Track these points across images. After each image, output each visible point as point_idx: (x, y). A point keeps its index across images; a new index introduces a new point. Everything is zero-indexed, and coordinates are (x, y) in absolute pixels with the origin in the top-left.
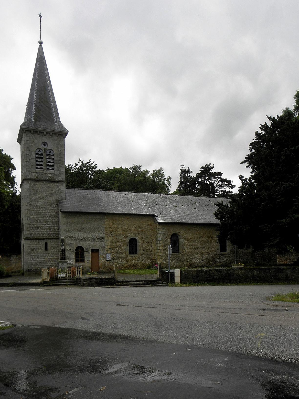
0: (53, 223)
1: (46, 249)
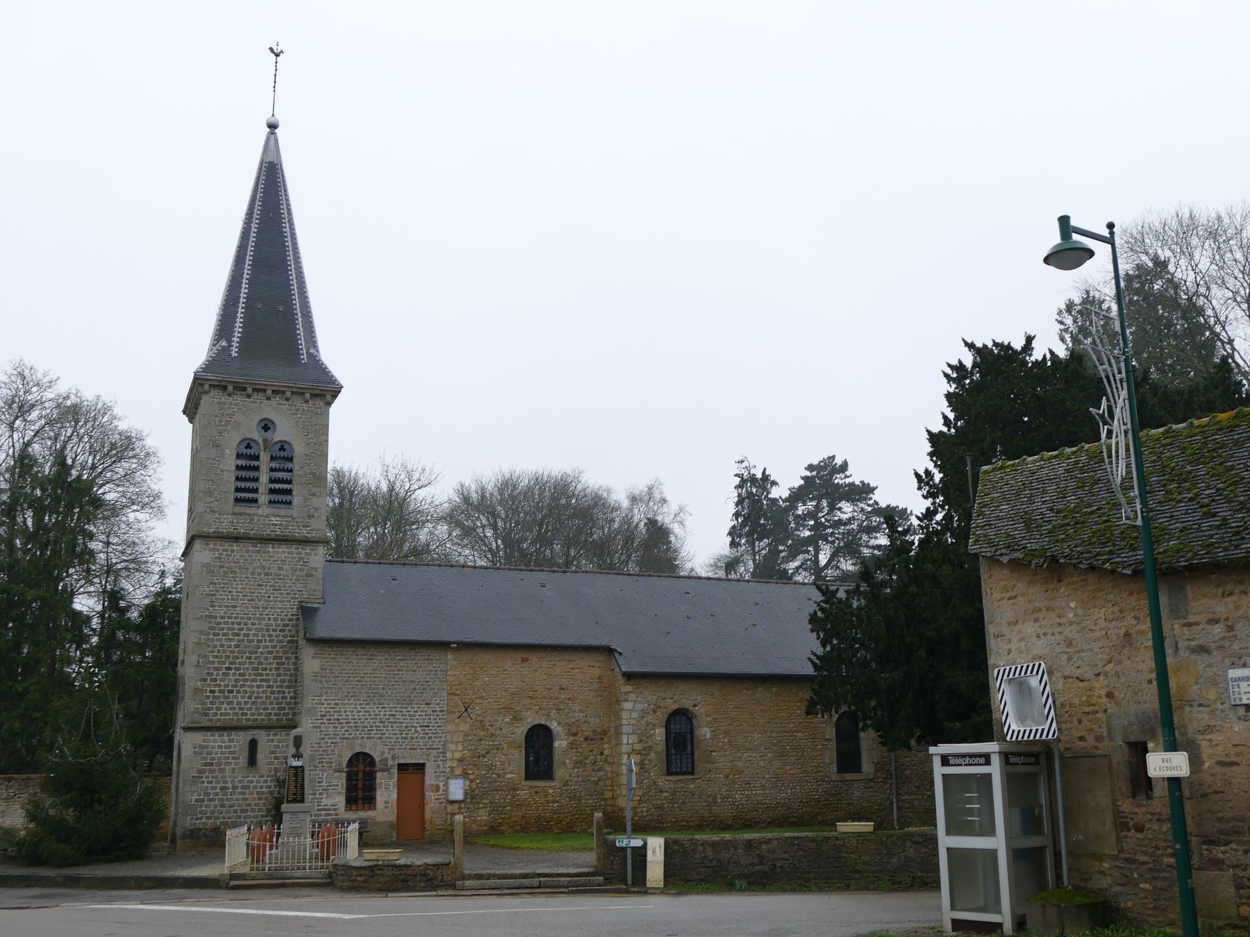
0: (279, 675)
1: (252, 761)
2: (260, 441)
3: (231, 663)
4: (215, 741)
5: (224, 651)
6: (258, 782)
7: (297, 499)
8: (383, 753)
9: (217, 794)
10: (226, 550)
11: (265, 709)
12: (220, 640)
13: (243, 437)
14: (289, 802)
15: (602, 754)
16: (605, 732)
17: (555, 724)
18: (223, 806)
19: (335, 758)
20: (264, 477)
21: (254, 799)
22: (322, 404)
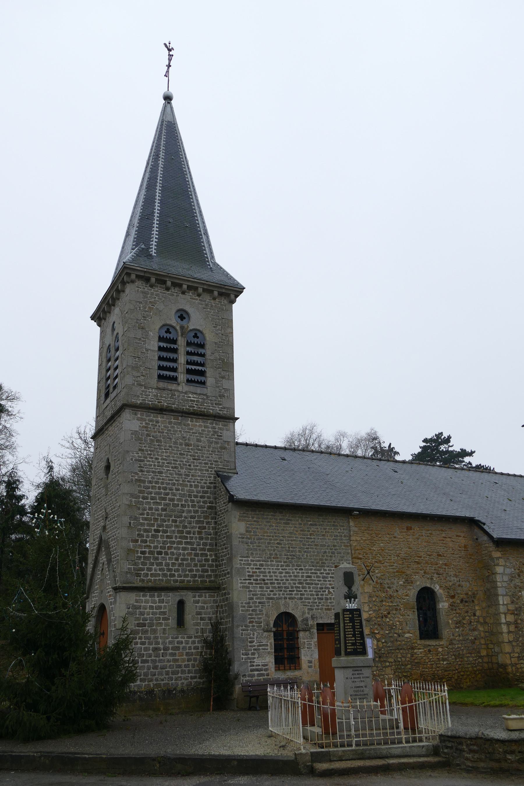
0: (201, 538)
1: (181, 622)
2: (178, 328)
3: (159, 526)
4: (147, 602)
5: (153, 514)
6: (187, 642)
7: (210, 381)
8: (304, 613)
9: (150, 656)
10: (152, 421)
11: (190, 571)
12: (149, 503)
13: (163, 323)
14: (347, 654)
15: (475, 615)
16: (474, 595)
17: (438, 587)
18: (155, 667)
19: (263, 617)
20: (182, 359)
21: (183, 661)
22: (226, 302)
